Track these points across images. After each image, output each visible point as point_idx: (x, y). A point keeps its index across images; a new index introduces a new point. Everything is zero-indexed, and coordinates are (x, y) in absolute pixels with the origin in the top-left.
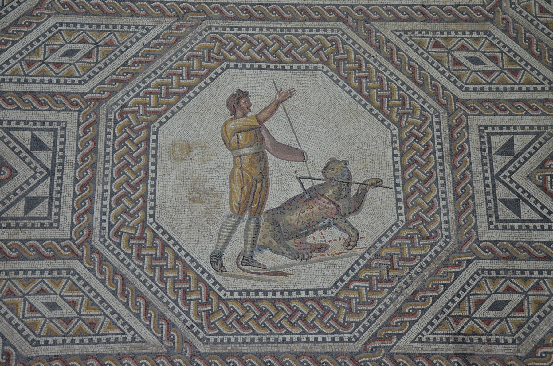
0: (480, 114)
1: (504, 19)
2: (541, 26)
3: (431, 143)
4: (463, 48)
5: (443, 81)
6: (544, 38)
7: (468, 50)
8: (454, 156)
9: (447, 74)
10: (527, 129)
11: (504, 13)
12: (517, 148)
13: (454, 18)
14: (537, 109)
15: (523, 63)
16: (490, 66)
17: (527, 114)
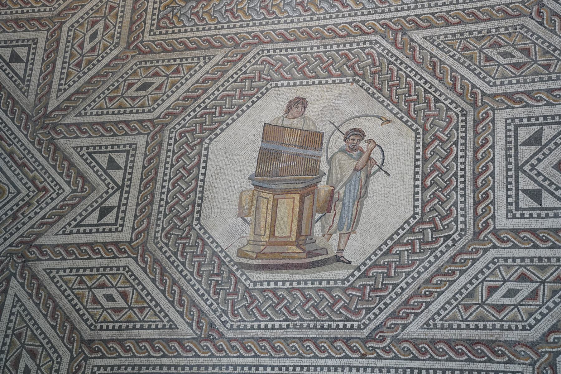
0: (47, 39)
1: (127, 56)
2: (116, 84)
3: (29, 5)
4: (106, 27)
5: (80, 14)
6: (106, 86)
7: (104, 30)
8: (16, 21)
9: (86, 16)
10: (29, 72)
11: (133, 57)
12: (15, 65)
13: (133, 20)
14: (44, 79)
15: (86, 70)
16: (87, 47)
17: (41, 72)
